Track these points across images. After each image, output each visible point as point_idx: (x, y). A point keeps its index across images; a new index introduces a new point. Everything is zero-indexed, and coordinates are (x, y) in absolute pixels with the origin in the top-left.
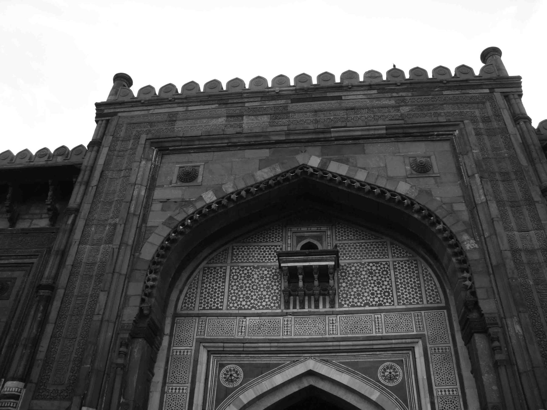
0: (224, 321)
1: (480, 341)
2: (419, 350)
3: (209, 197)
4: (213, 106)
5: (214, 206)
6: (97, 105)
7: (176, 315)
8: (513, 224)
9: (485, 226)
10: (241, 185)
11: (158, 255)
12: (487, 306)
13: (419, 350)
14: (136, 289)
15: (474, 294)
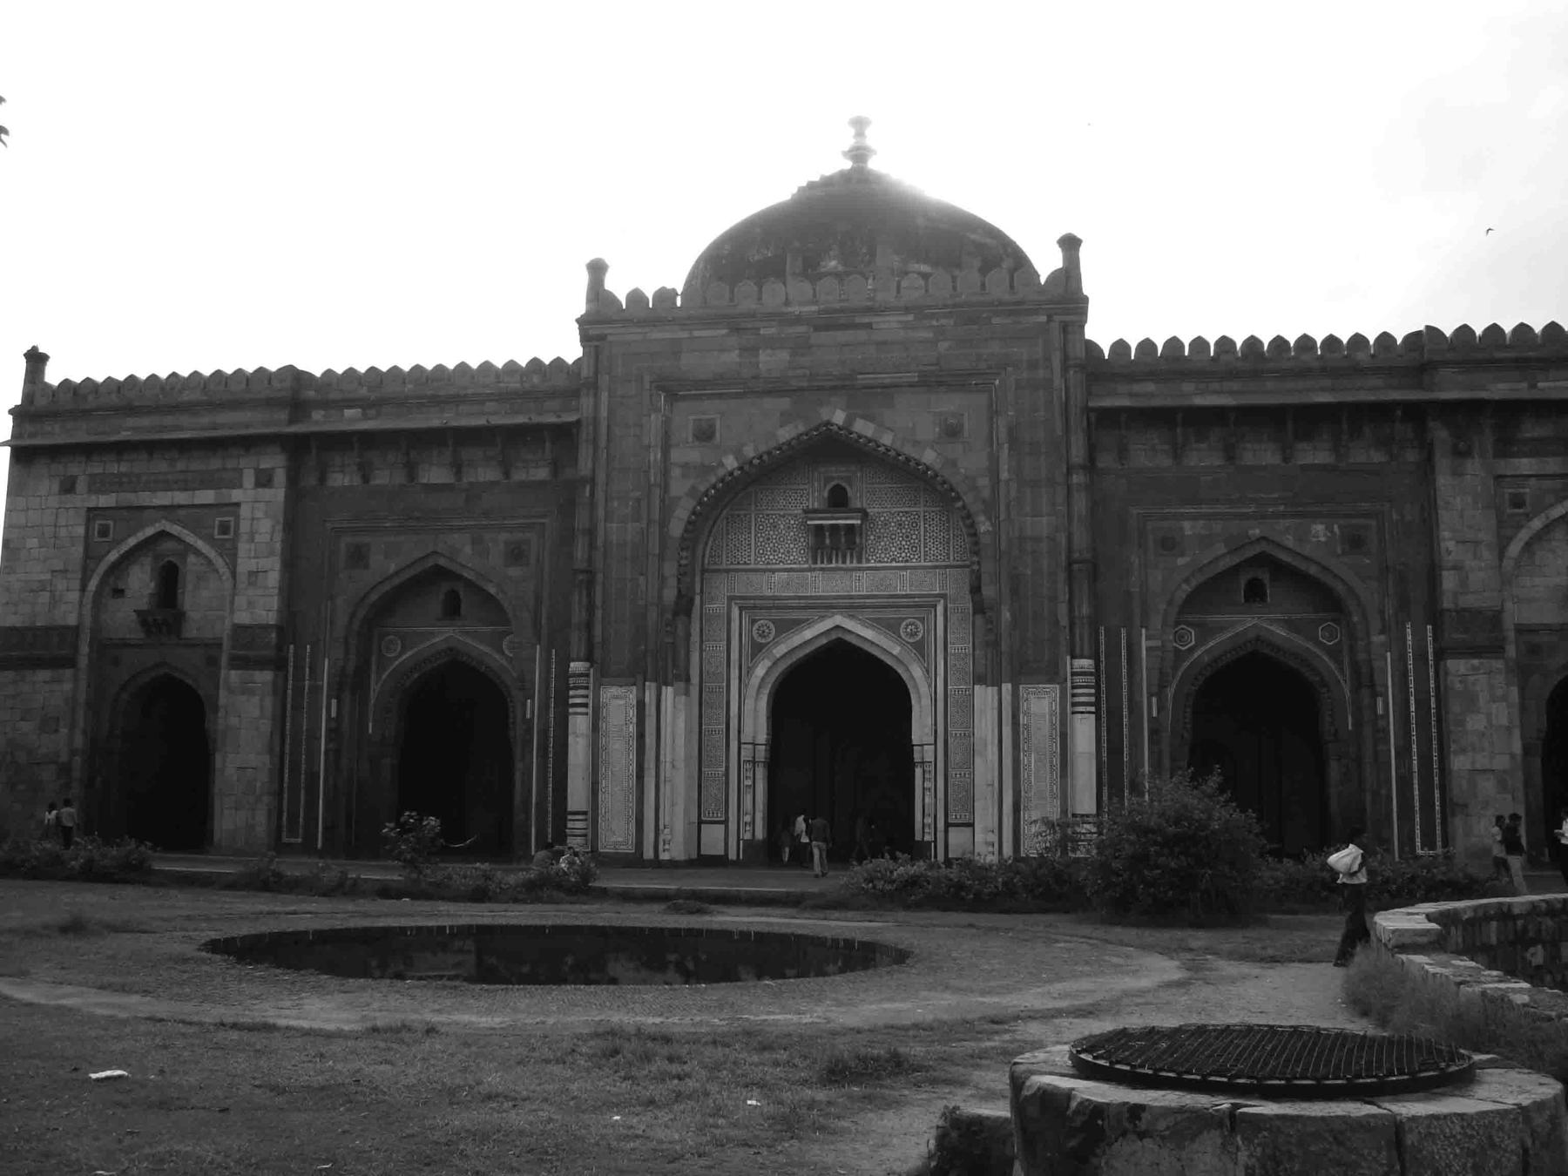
0: (752, 576)
1: (979, 617)
2: (940, 609)
3: (731, 463)
4: (724, 332)
5: (737, 473)
6: (578, 321)
7: (703, 571)
8: (1028, 509)
9: (1002, 508)
10: (763, 448)
11: (686, 531)
12: (988, 591)
13: (940, 609)
14: (670, 569)
15: (979, 578)
